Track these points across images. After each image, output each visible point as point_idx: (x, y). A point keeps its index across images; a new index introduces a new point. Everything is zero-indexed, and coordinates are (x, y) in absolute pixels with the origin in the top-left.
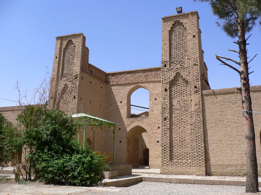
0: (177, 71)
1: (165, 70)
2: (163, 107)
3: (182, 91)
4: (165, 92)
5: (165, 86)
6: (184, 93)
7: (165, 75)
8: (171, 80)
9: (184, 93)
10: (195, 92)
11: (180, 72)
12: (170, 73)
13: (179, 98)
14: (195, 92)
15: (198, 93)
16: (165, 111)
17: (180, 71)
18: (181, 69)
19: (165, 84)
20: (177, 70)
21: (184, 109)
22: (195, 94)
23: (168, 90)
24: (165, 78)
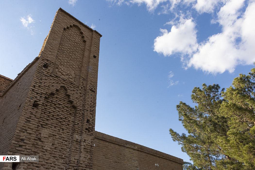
0: (63, 85)
1: (44, 72)
2: (18, 137)
3: (61, 118)
4: (33, 109)
5: (36, 97)
6: (64, 123)
7: (41, 79)
8: (50, 92)
9: (64, 123)
10: (86, 129)
11: (67, 88)
12: (52, 81)
13: (55, 129)
14: (86, 129)
15: (91, 132)
16: (20, 146)
17: (68, 88)
18: (69, 85)
19: (37, 93)
20: (64, 83)
21: (58, 153)
22: (86, 132)
23: (40, 107)
24: (40, 85)
